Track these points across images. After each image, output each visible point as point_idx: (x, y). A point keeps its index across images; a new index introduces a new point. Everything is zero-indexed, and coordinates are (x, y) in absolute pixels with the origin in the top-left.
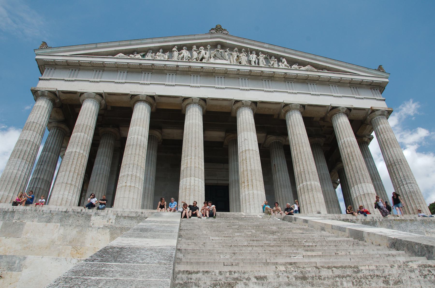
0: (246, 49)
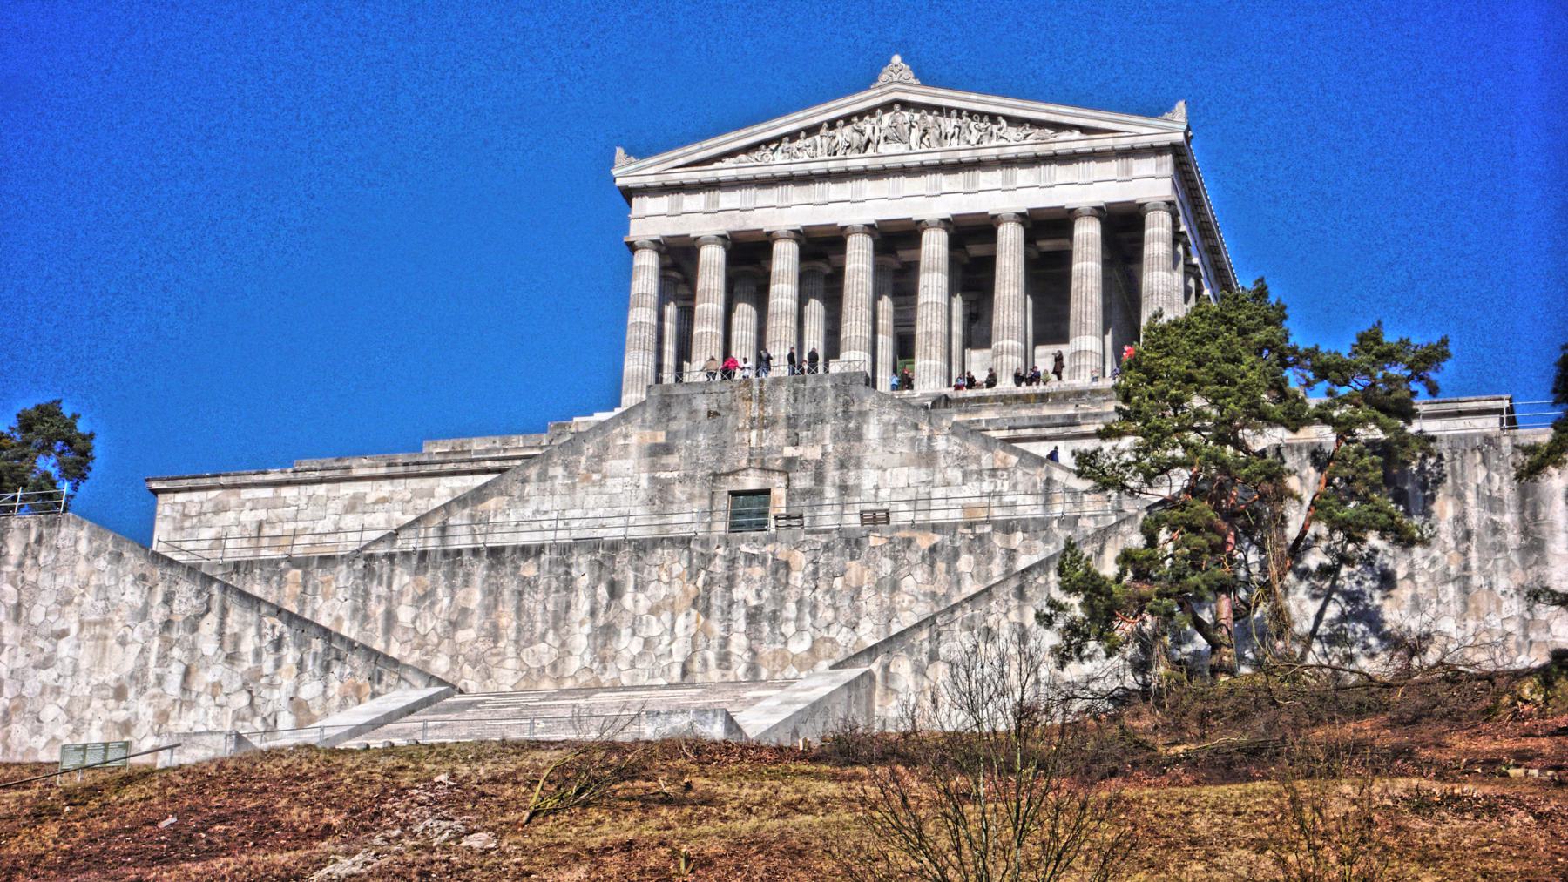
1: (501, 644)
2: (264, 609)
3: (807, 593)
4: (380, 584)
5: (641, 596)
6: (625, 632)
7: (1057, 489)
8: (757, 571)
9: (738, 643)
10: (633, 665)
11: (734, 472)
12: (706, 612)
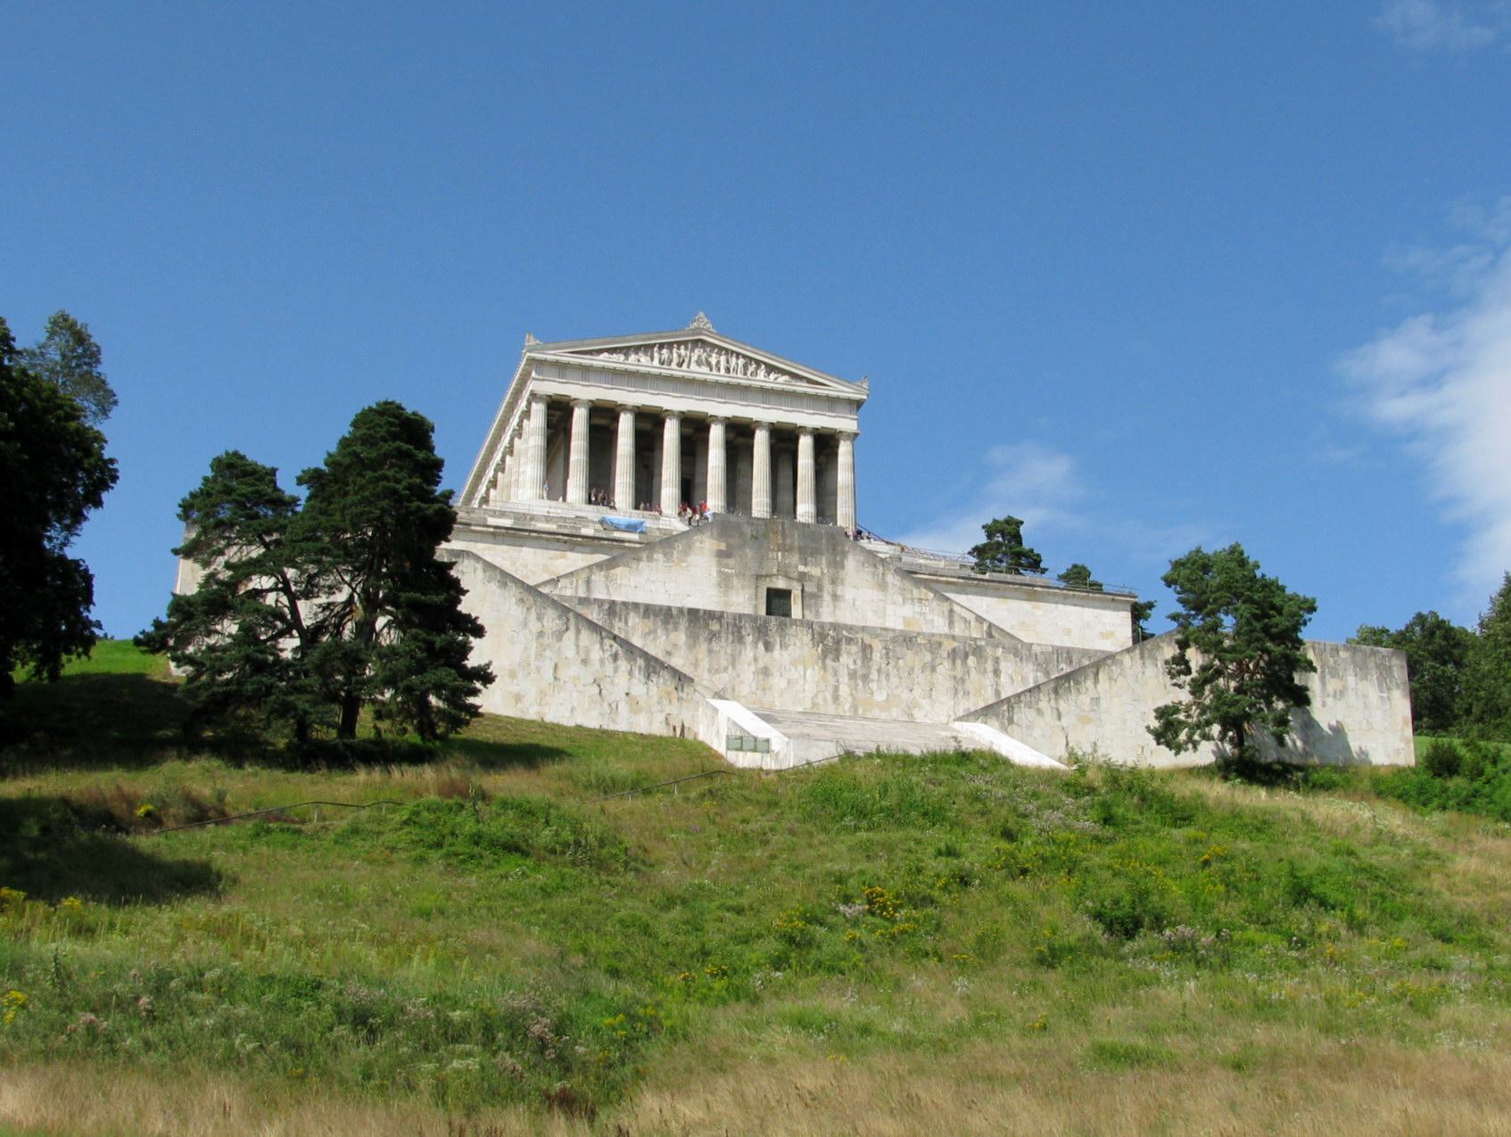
0: (727, 350)
1: (699, 670)
2: (604, 634)
3: (883, 666)
4: (620, 620)
5: (784, 652)
6: (777, 674)
7: (956, 618)
8: (854, 649)
9: (844, 690)
10: (781, 696)
11: (771, 576)
12: (824, 667)
